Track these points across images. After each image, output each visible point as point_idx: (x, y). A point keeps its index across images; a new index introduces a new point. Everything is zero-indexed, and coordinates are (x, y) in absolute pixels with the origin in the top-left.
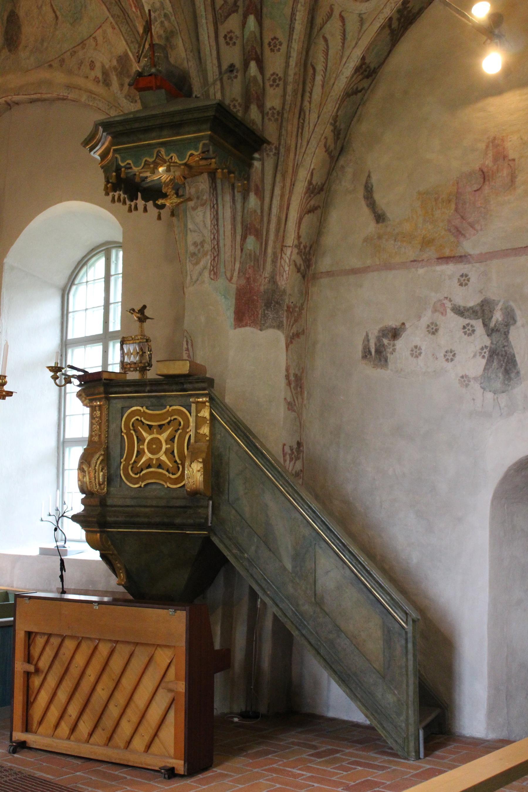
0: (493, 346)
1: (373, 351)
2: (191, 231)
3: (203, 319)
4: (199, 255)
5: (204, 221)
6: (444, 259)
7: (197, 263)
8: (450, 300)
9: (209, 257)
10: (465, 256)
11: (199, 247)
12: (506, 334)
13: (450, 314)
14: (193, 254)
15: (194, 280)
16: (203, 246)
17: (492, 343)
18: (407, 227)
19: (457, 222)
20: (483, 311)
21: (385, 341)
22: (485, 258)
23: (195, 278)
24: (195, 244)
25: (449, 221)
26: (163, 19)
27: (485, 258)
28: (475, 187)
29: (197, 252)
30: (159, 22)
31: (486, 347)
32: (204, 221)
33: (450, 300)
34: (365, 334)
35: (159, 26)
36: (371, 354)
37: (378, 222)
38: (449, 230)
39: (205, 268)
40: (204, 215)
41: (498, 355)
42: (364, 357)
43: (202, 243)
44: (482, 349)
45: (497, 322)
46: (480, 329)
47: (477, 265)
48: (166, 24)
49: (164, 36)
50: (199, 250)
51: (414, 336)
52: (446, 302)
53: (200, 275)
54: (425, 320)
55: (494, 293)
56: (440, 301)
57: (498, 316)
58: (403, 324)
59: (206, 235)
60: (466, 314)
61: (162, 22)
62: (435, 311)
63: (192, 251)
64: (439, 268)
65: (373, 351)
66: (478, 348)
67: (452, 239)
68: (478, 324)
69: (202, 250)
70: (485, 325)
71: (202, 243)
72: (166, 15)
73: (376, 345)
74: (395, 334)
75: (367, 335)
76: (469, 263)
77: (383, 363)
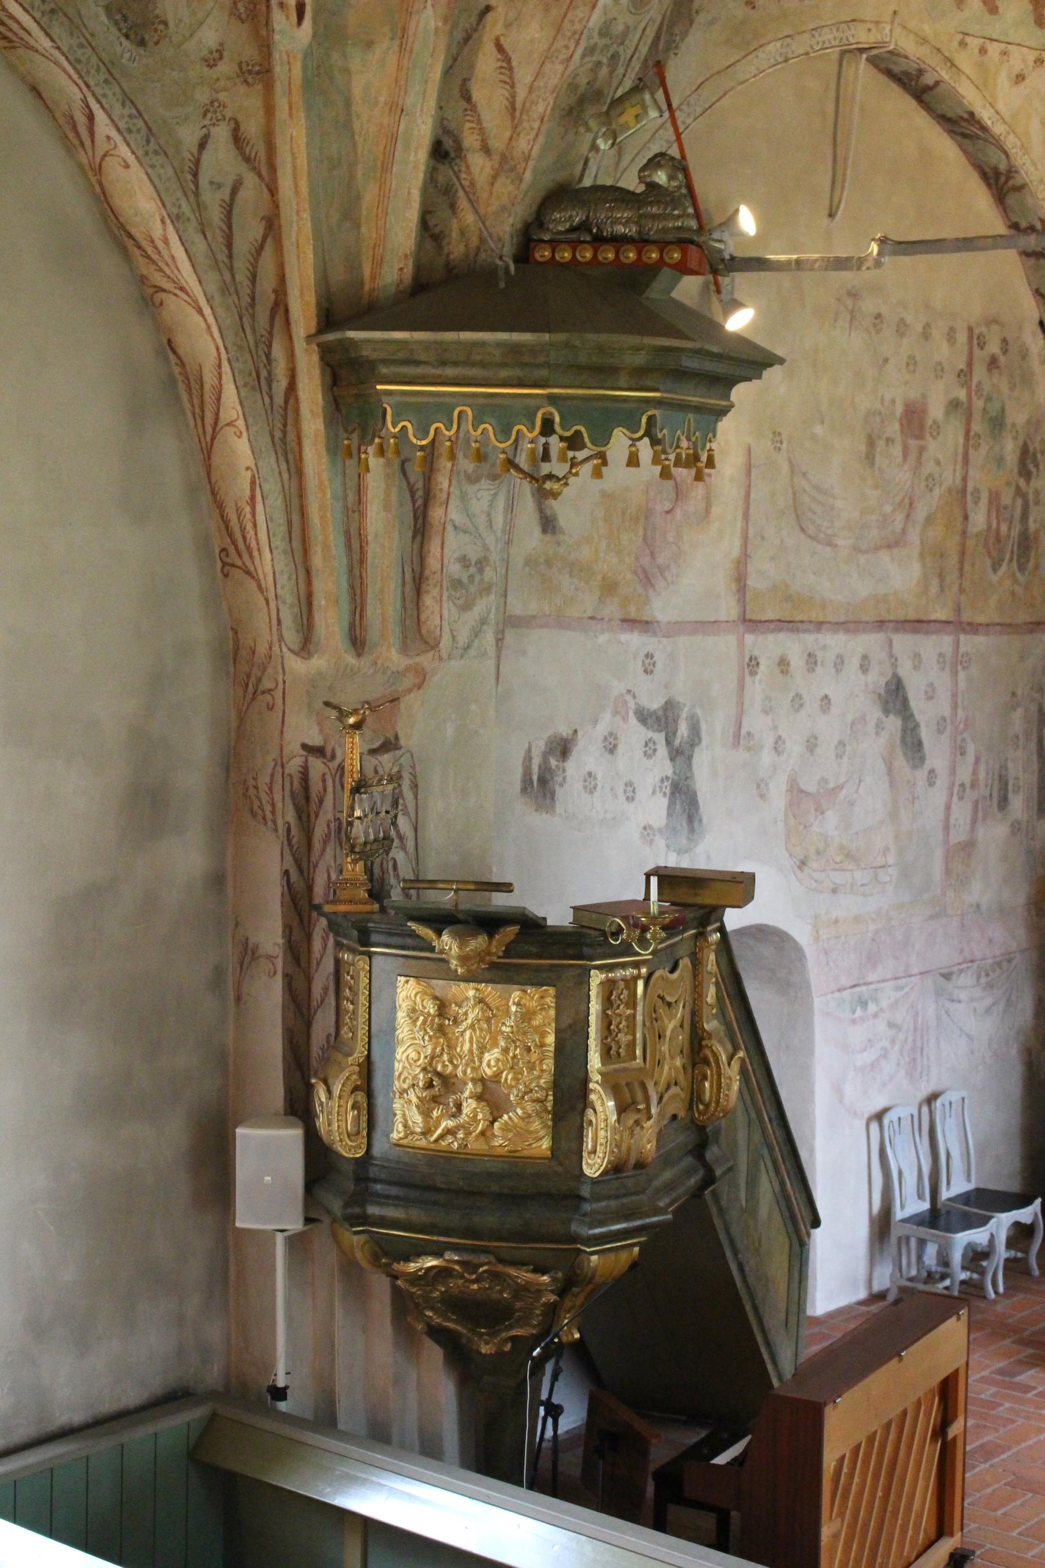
0: (676, 777)
1: (535, 778)
2: (455, 527)
3: (450, 731)
4: (472, 589)
5: (489, 515)
6: (631, 623)
7: (467, 607)
8: (634, 697)
9: (492, 597)
10: (652, 622)
11: (473, 570)
12: (690, 758)
13: (633, 720)
14: (457, 584)
15: (461, 645)
16: (481, 571)
17: (674, 772)
18: (585, 553)
19: (646, 560)
20: (661, 718)
21: (553, 762)
22: (677, 628)
23: (463, 638)
24: (464, 561)
25: (637, 559)
26: (605, 60)
27: (677, 628)
28: (668, 506)
29: (465, 580)
30: (594, 58)
31: (667, 778)
32: (489, 515)
33: (634, 697)
34: (526, 746)
35: (589, 66)
36: (532, 786)
37: (544, 531)
38: (635, 573)
39: (484, 621)
40: (492, 501)
41: (679, 792)
42: (524, 790)
43: (481, 564)
44: (662, 781)
45: (682, 738)
46: (662, 751)
47: (665, 640)
48: (604, 71)
49: (581, 90)
50: (471, 577)
51: (586, 757)
52: (628, 698)
53: (476, 636)
54: (602, 728)
55: (681, 692)
56: (622, 695)
57: (683, 730)
58: (576, 731)
59: (492, 548)
60: (649, 721)
61: (599, 64)
62: (616, 713)
63: (456, 576)
64: (625, 637)
65: (535, 778)
66: (658, 779)
67: (640, 590)
68: (660, 738)
69: (477, 579)
70: (669, 742)
71: (481, 564)
72: (615, 57)
73: (540, 767)
74: (563, 748)
75: (529, 750)
76: (655, 634)
77: (548, 801)
